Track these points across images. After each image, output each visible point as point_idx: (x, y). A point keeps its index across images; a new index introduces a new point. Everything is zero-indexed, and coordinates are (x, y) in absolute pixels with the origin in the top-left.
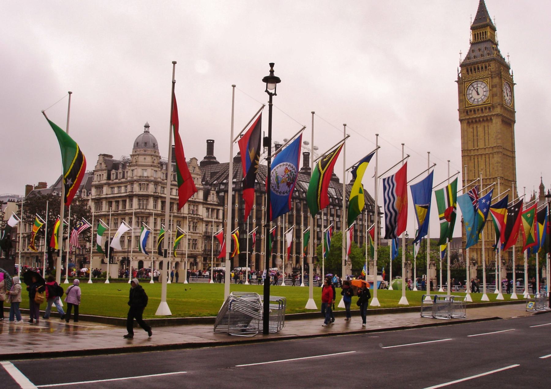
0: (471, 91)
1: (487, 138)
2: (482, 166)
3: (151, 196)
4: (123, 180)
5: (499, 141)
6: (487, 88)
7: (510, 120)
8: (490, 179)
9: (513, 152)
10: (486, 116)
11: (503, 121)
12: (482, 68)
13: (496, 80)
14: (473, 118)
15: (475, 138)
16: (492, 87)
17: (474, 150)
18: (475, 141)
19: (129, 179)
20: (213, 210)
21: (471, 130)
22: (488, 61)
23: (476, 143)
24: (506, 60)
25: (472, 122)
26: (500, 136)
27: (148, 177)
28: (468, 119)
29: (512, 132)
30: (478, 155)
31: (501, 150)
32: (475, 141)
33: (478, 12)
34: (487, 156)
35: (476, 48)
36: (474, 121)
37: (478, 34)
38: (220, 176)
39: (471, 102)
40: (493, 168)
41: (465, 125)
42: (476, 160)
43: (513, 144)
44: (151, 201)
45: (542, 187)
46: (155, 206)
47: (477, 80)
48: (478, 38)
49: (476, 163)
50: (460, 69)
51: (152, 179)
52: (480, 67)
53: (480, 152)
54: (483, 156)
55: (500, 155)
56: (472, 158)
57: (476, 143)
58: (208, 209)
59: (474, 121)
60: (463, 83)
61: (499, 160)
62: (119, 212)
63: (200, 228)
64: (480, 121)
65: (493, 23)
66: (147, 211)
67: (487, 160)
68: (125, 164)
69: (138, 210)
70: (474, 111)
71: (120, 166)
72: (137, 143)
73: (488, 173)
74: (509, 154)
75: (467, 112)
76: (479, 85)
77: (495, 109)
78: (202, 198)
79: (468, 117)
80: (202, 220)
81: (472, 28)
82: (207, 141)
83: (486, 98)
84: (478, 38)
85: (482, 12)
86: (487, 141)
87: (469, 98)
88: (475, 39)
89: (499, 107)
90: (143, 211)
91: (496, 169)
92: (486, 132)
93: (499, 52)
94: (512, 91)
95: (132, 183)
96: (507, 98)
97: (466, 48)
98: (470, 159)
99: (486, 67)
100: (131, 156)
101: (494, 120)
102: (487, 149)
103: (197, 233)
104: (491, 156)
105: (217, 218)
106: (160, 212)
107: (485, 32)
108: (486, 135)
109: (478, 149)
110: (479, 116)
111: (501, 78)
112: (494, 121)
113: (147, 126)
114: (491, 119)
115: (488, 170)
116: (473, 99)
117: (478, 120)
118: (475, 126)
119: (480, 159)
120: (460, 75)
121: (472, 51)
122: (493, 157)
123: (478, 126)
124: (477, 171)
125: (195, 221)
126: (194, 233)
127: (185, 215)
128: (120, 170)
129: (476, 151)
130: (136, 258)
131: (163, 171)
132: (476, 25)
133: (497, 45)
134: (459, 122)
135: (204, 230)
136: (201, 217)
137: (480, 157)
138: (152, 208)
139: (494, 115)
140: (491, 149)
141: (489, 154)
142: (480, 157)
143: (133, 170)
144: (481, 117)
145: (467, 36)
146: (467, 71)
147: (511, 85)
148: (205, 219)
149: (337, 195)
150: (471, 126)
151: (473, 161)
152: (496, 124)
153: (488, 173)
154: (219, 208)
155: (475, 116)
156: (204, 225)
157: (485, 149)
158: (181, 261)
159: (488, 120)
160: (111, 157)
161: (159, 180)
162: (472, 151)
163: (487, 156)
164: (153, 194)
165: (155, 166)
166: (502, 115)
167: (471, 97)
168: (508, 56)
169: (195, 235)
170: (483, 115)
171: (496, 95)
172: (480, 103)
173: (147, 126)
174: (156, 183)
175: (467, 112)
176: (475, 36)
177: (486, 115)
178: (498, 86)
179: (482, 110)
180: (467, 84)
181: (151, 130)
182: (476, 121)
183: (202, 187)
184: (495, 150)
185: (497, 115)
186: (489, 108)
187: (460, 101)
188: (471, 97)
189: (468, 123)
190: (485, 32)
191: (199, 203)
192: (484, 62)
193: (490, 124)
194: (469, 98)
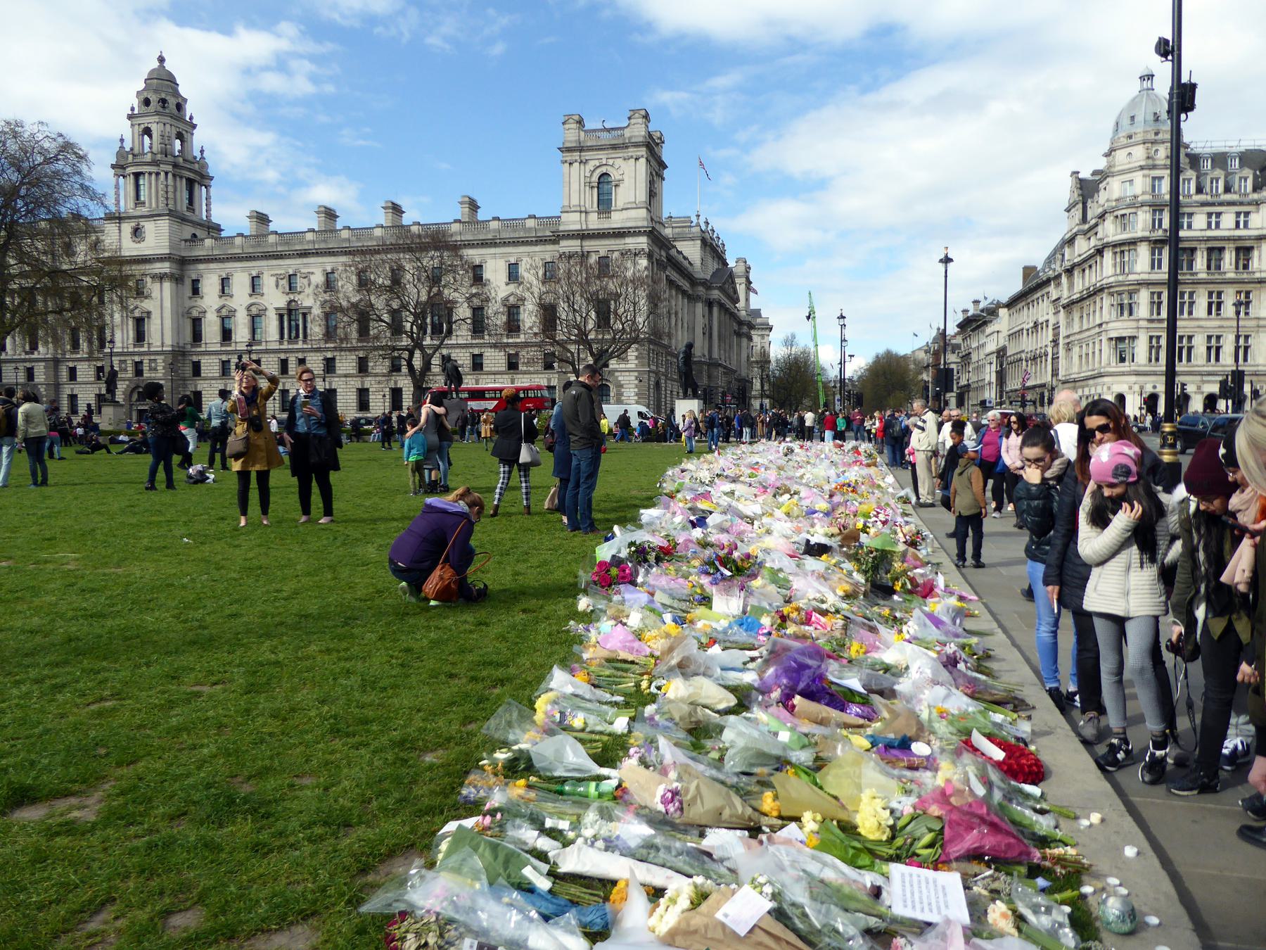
66: (1131, 277)
90: (1121, 278)
130: (1109, 388)
138: (1147, 268)
164: (1147, 234)
165: (1154, 167)
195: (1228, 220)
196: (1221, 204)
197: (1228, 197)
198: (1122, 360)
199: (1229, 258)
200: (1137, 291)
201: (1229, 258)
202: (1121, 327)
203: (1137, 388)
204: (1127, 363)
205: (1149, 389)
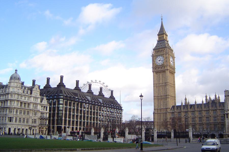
1: (163, 79)
3: (15, 100)
4: (5, 93)
9: (174, 85)
11: (169, 72)
12: (162, 51)
14: (158, 71)
15: (159, 79)
18: (159, 80)
19: (7, 92)
20: (44, 107)
24: (172, 48)
27: (15, 92)
32: (159, 80)
33: (160, 29)
38: (51, 93)
40: (166, 91)
41: (155, 73)
44: (16, 102)
45: (186, 99)
46: (18, 104)
47: (159, 55)
49: (159, 89)
50: (153, 51)
51: (17, 93)
58: (42, 106)
60: (154, 57)
62: (2, 107)
63: (38, 114)
68: (6, 86)
69: (10, 106)
70: (158, 68)
71: (5, 87)
72: (11, 78)
73: (164, 93)
74: (172, 85)
75: (155, 68)
78: (40, 102)
79: (155, 71)
80: (39, 111)
81: (158, 35)
82: (47, 78)
83: (163, 63)
85: (162, 29)
87: (156, 63)
92: (163, 76)
93: (169, 44)
94: (174, 60)
95: (8, 94)
96: (172, 63)
99: (163, 50)
100: (8, 82)
101: (167, 72)
103: (36, 117)
105: (46, 110)
106: (20, 107)
113: (16, 71)
114: (165, 71)
115: (164, 92)
116: (158, 63)
120: (153, 53)
121: (158, 44)
124: (159, 92)
125: (36, 111)
126: (35, 117)
127: (31, 109)
128: (4, 89)
131: (22, 89)
132: (160, 34)
133: (168, 42)
134: (152, 72)
135: (40, 115)
136: (39, 110)
143: (9, 89)
145: (157, 38)
146: (156, 52)
148: (40, 111)
149: (103, 102)
150: (157, 74)
153: (164, 93)
154: (47, 106)
155: (158, 70)
159: (164, 71)
160: (2, 83)
161: (20, 93)
164: (16, 99)
165: (18, 87)
169: (35, 117)
172: (160, 65)
173: (16, 71)
174: (18, 94)
175: (155, 68)
176: (159, 38)
181: (18, 72)
183: (40, 97)
187: (153, 64)
189: (156, 72)
191: (38, 104)
192: (162, 48)
195: (27, 98)
196: (26, 96)
197: (27, 95)
198: (10, 121)
199: (27, 105)
200: (14, 109)
201: (27, 105)
202: (11, 115)
203: (13, 127)
204: (11, 122)
205: (15, 127)
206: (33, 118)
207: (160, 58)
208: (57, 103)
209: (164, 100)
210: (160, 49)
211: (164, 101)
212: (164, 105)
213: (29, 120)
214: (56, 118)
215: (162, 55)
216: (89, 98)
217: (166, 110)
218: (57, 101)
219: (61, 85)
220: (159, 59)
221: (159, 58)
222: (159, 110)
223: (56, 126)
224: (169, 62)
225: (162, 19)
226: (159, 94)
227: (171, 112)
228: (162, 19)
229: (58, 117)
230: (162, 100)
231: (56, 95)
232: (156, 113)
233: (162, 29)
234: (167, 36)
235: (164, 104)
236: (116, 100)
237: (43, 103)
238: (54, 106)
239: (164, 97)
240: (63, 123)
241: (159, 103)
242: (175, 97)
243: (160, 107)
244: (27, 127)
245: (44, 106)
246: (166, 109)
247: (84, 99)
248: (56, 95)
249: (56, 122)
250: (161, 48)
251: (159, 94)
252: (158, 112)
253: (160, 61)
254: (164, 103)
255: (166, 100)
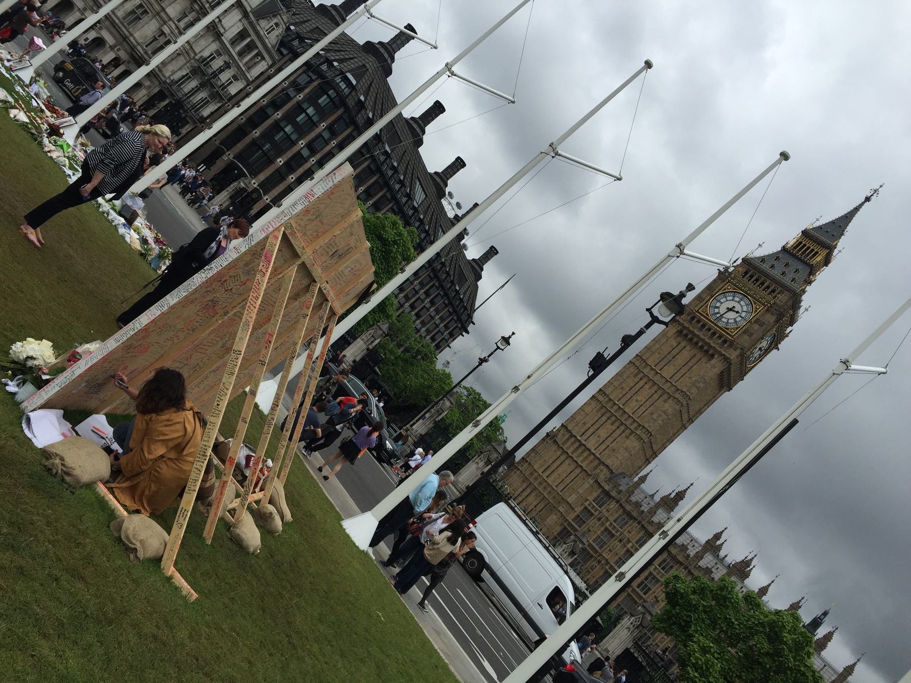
0: (724, 299)
1: (683, 371)
2: (642, 397)
5: (694, 390)
6: (749, 317)
7: (729, 382)
8: (635, 421)
10: (710, 346)
12: (768, 287)
13: (770, 318)
14: (692, 333)
16: (756, 322)
17: (652, 369)
18: (666, 360)
21: (675, 344)
22: (783, 286)
23: (663, 363)
25: (686, 335)
26: (701, 385)
28: (685, 327)
29: (714, 398)
30: (650, 380)
31: (685, 403)
32: (666, 360)
33: (833, 222)
34: (660, 392)
35: (785, 258)
36: (690, 336)
37: (805, 245)
39: (710, 311)
42: (641, 383)
43: (700, 412)
48: (799, 251)
49: (638, 387)
50: (739, 262)
52: (766, 284)
53: (656, 379)
54: (655, 388)
55: (678, 408)
56: (641, 375)
57: (663, 363)
59: (690, 336)
61: (670, 411)
64: (697, 343)
65: (834, 254)
67: (656, 396)
70: (703, 326)
74: (685, 417)
75: (693, 318)
76: (742, 303)
77: (732, 350)
79: (686, 325)
81: (805, 233)
84: (799, 251)
85: (839, 225)
86: (679, 375)
87: (713, 304)
88: (795, 248)
89: (738, 352)
91: (655, 416)
92: (690, 364)
94: (767, 351)
96: (757, 353)
97: (772, 247)
98: (636, 375)
102: (668, 384)
104: (666, 396)
107: (817, 253)
108: (686, 368)
109: (657, 373)
110: (702, 337)
111: (777, 321)
112: (713, 361)
114: (712, 356)
116: (717, 310)
117: (695, 340)
118: (683, 344)
119: (647, 386)
121: (776, 257)
122: (665, 401)
123: (688, 348)
124: (629, 396)
129: (653, 373)
135: (206, 54)
136: (222, 31)
137: (650, 383)
139: (721, 355)
140: (673, 389)
141: (664, 392)
142: (650, 383)
144: (703, 340)
145: (790, 235)
146: (746, 273)
147: (775, 344)
150: (679, 339)
151: (637, 380)
152: (714, 367)
156: (214, 47)
157: (667, 381)
158: (112, 48)
162: (648, 368)
163: (660, 392)
166: (730, 364)
167: (718, 307)
168: (807, 310)
170: (707, 340)
171: (751, 335)
175: (693, 318)
176: (798, 244)
177: (713, 345)
178: (764, 327)
179: (714, 334)
180: (729, 287)
182: (691, 340)
184: (677, 395)
185: (726, 359)
186: (725, 342)
188: (718, 307)
189: (680, 332)
190: (817, 253)
193: (704, 359)
194: (713, 304)
206: (166, 29)
207: (742, 303)
208: (307, 91)
209: (618, 432)
210: (768, 276)
211: (615, 435)
212: (603, 447)
213: (145, 18)
214: (257, 133)
215: (754, 300)
216: (419, 196)
217: (596, 468)
218: (316, 83)
219: (381, 55)
220: (730, 305)
221: (737, 299)
222: (572, 444)
223: (231, 156)
224: (753, 345)
225: (868, 199)
226: (623, 400)
227: (607, 487)
228: (868, 199)
229: (267, 136)
230: (614, 428)
231: (335, 64)
232: (555, 442)
233: (839, 225)
234: (827, 261)
235: (608, 442)
236: (477, 287)
237: (264, 25)
238: (291, 92)
239: (628, 423)
240: (262, 177)
241: (596, 427)
242: (655, 455)
243: (585, 437)
244: (111, 34)
245: (252, 41)
246: (596, 462)
247: (402, 178)
248: (335, 64)
249: (240, 146)
250: (773, 280)
251: (623, 400)
252: (563, 444)
253: (733, 311)
254: (610, 439)
255: (627, 437)
